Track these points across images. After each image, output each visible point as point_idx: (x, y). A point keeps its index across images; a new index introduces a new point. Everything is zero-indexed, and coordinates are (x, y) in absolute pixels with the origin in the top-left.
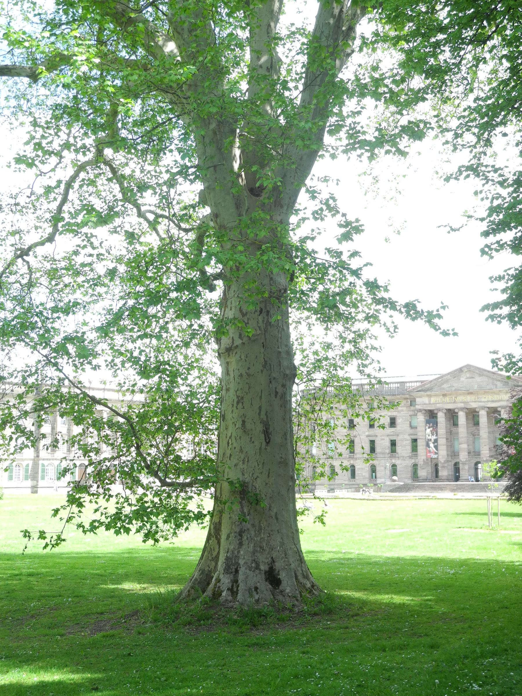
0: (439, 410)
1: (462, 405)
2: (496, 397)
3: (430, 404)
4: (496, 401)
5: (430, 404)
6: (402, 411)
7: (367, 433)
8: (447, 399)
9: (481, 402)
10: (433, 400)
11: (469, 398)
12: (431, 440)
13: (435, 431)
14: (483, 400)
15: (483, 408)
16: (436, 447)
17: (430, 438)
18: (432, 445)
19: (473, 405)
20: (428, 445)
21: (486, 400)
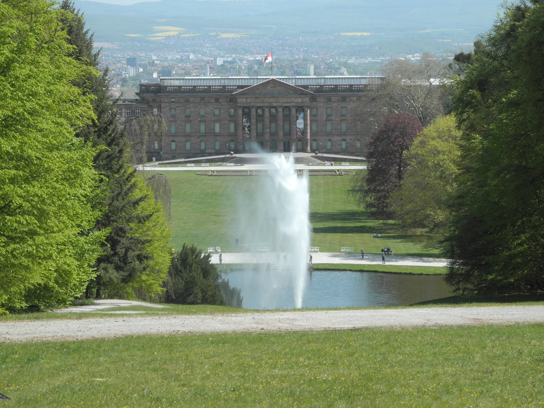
0: (253, 107)
1: (267, 104)
2: (289, 100)
3: (246, 103)
4: (289, 103)
5: (246, 103)
6: (224, 105)
7: (199, 119)
9: (279, 103)
10: (249, 100)
11: (272, 100)
13: (249, 120)
14: (281, 101)
15: (281, 107)
16: (249, 130)
17: (245, 124)
18: (246, 129)
19: (275, 105)
20: (244, 129)
21: (282, 102)
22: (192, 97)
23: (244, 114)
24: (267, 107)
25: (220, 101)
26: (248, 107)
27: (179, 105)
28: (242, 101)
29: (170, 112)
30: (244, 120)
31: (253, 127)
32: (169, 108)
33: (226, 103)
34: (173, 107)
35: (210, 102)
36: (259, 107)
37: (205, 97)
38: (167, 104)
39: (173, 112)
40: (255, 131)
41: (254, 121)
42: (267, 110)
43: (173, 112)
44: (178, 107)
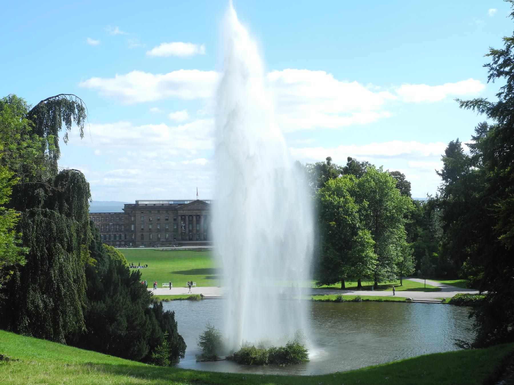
0: (187, 215)
1: (195, 214)
6: (171, 214)
7: (157, 223)
8: (190, 212)
10: (184, 212)
11: (197, 212)
12: (183, 226)
13: (185, 223)
17: (182, 225)
18: (183, 228)
20: (182, 228)
22: (153, 210)
23: (182, 219)
24: (195, 215)
25: (169, 212)
26: (184, 216)
27: (146, 214)
28: (180, 212)
29: (141, 218)
30: (182, 222)
31: (187, 226)
32: (140, 216)
33: (171, 214)
34: (142, 216)
35: (163, 213)
36: (190, 216)
37: (160, 210)
38: (139, 214)
39: (142, 219)
40: (188, 229)
41: (187, 223)
42: (194, 217)
43: (142, 219)
44: (145, 215)
